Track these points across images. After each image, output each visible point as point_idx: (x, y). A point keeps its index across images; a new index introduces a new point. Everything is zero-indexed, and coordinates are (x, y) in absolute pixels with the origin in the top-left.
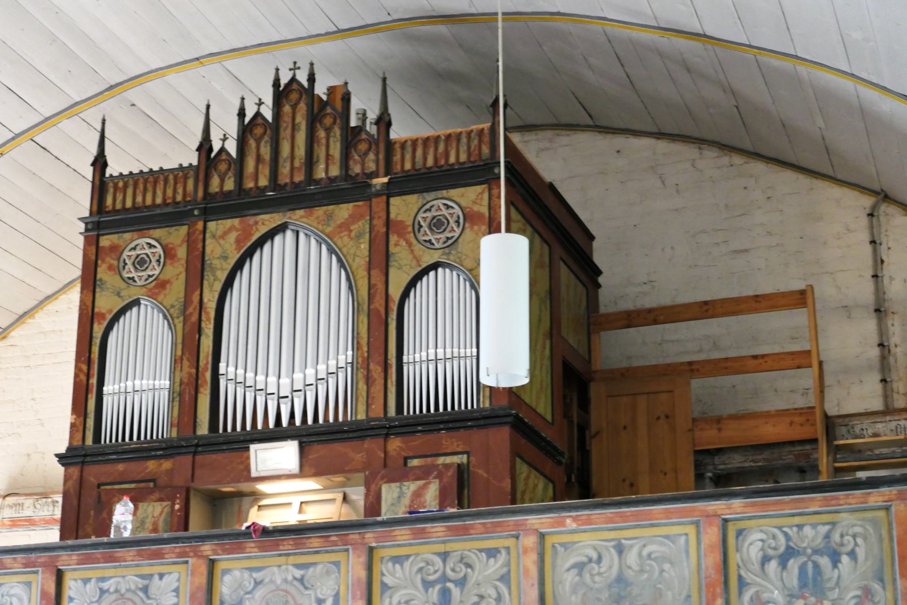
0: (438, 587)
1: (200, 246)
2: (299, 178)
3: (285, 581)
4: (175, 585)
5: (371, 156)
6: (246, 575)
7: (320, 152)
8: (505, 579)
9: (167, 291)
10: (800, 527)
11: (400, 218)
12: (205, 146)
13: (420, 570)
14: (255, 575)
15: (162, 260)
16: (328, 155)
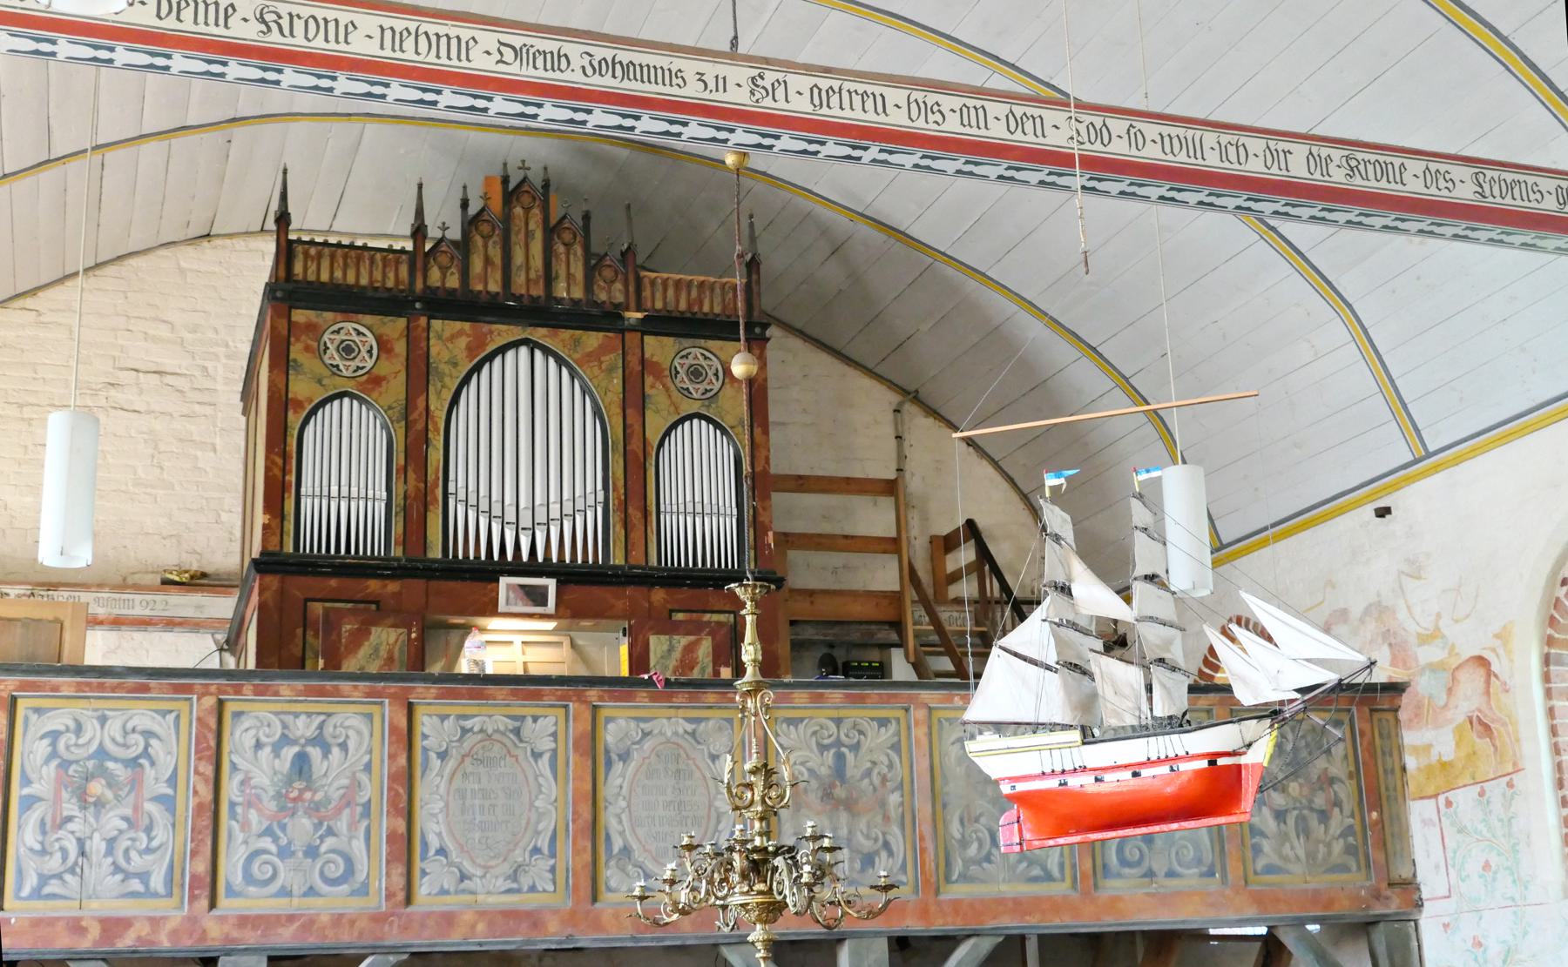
0: (832, 751)
1: (424, 344)
2: (538, 291)
3: (676, 733)
4: (553, 729)
6: (633, 724)
7: (560, 269)
8: (896, 747)
9: (383, 389)
13: (815, 733)
14: (642, 725)
15: (375, 352)
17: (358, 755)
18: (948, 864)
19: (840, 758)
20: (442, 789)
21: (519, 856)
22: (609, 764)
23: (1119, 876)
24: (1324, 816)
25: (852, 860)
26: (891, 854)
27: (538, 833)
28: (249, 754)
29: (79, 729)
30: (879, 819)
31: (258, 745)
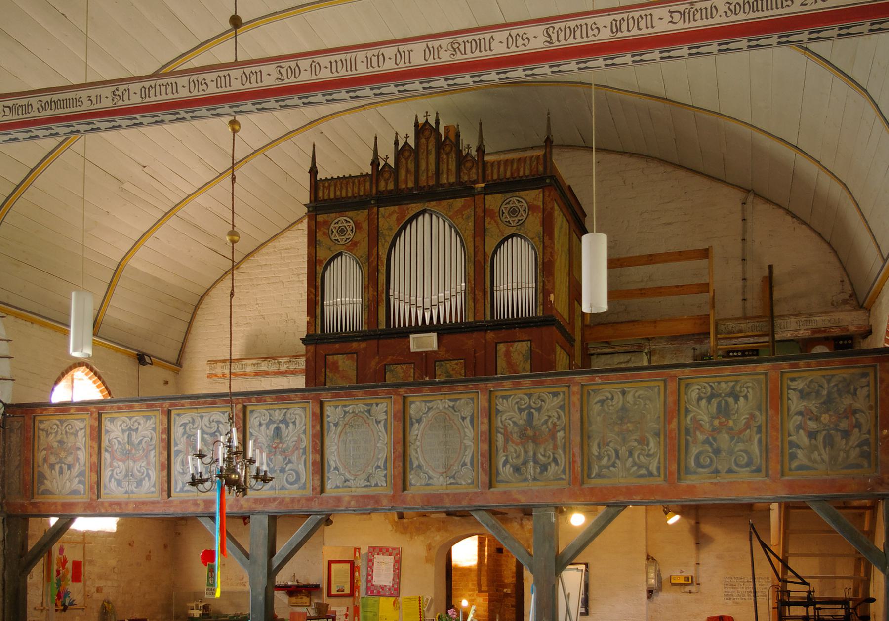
3: (445, 408)
5: (474, 170)
6: (423, 404)
8: (562, 407)
10: (719, 383)
11: (491, 208)
12: (375, 163)
13: (517, 403)
16: (448, 169)
17: (300, 427)
18: (590, 468)
19: (530, 415)
20: (336, 441)
21: (370, 470)
22: (412, 424)
23: (695, 473)
24: (846, 434)
25: (535, 468)
26: (557, 464)
27: (378, 459)
28: (257, 429)
29: (193, 422)
30: (551, 446)
31: (260, 424)
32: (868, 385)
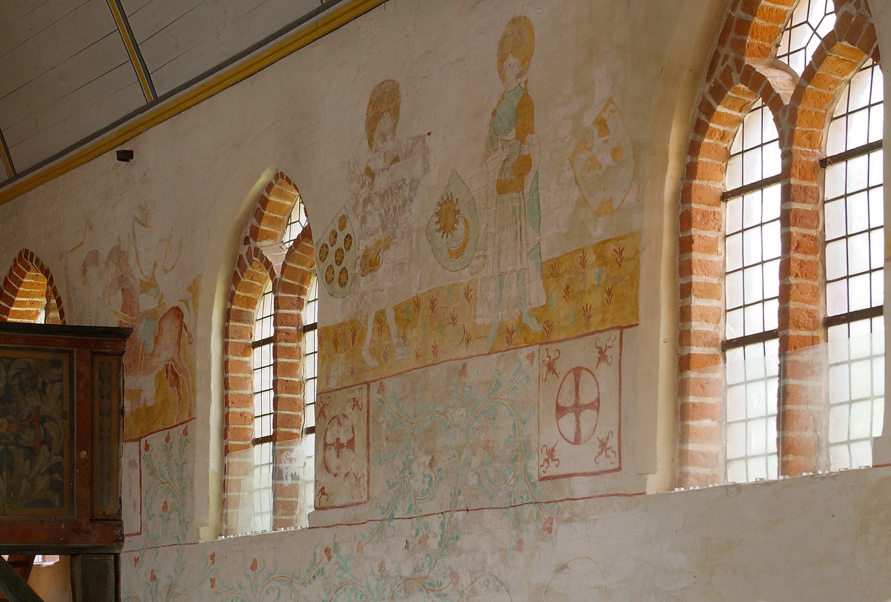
32: (61, 380)
